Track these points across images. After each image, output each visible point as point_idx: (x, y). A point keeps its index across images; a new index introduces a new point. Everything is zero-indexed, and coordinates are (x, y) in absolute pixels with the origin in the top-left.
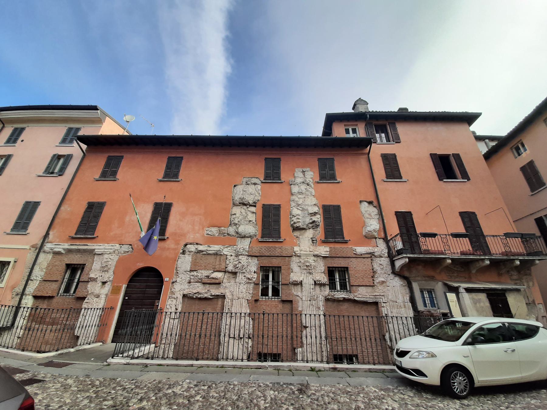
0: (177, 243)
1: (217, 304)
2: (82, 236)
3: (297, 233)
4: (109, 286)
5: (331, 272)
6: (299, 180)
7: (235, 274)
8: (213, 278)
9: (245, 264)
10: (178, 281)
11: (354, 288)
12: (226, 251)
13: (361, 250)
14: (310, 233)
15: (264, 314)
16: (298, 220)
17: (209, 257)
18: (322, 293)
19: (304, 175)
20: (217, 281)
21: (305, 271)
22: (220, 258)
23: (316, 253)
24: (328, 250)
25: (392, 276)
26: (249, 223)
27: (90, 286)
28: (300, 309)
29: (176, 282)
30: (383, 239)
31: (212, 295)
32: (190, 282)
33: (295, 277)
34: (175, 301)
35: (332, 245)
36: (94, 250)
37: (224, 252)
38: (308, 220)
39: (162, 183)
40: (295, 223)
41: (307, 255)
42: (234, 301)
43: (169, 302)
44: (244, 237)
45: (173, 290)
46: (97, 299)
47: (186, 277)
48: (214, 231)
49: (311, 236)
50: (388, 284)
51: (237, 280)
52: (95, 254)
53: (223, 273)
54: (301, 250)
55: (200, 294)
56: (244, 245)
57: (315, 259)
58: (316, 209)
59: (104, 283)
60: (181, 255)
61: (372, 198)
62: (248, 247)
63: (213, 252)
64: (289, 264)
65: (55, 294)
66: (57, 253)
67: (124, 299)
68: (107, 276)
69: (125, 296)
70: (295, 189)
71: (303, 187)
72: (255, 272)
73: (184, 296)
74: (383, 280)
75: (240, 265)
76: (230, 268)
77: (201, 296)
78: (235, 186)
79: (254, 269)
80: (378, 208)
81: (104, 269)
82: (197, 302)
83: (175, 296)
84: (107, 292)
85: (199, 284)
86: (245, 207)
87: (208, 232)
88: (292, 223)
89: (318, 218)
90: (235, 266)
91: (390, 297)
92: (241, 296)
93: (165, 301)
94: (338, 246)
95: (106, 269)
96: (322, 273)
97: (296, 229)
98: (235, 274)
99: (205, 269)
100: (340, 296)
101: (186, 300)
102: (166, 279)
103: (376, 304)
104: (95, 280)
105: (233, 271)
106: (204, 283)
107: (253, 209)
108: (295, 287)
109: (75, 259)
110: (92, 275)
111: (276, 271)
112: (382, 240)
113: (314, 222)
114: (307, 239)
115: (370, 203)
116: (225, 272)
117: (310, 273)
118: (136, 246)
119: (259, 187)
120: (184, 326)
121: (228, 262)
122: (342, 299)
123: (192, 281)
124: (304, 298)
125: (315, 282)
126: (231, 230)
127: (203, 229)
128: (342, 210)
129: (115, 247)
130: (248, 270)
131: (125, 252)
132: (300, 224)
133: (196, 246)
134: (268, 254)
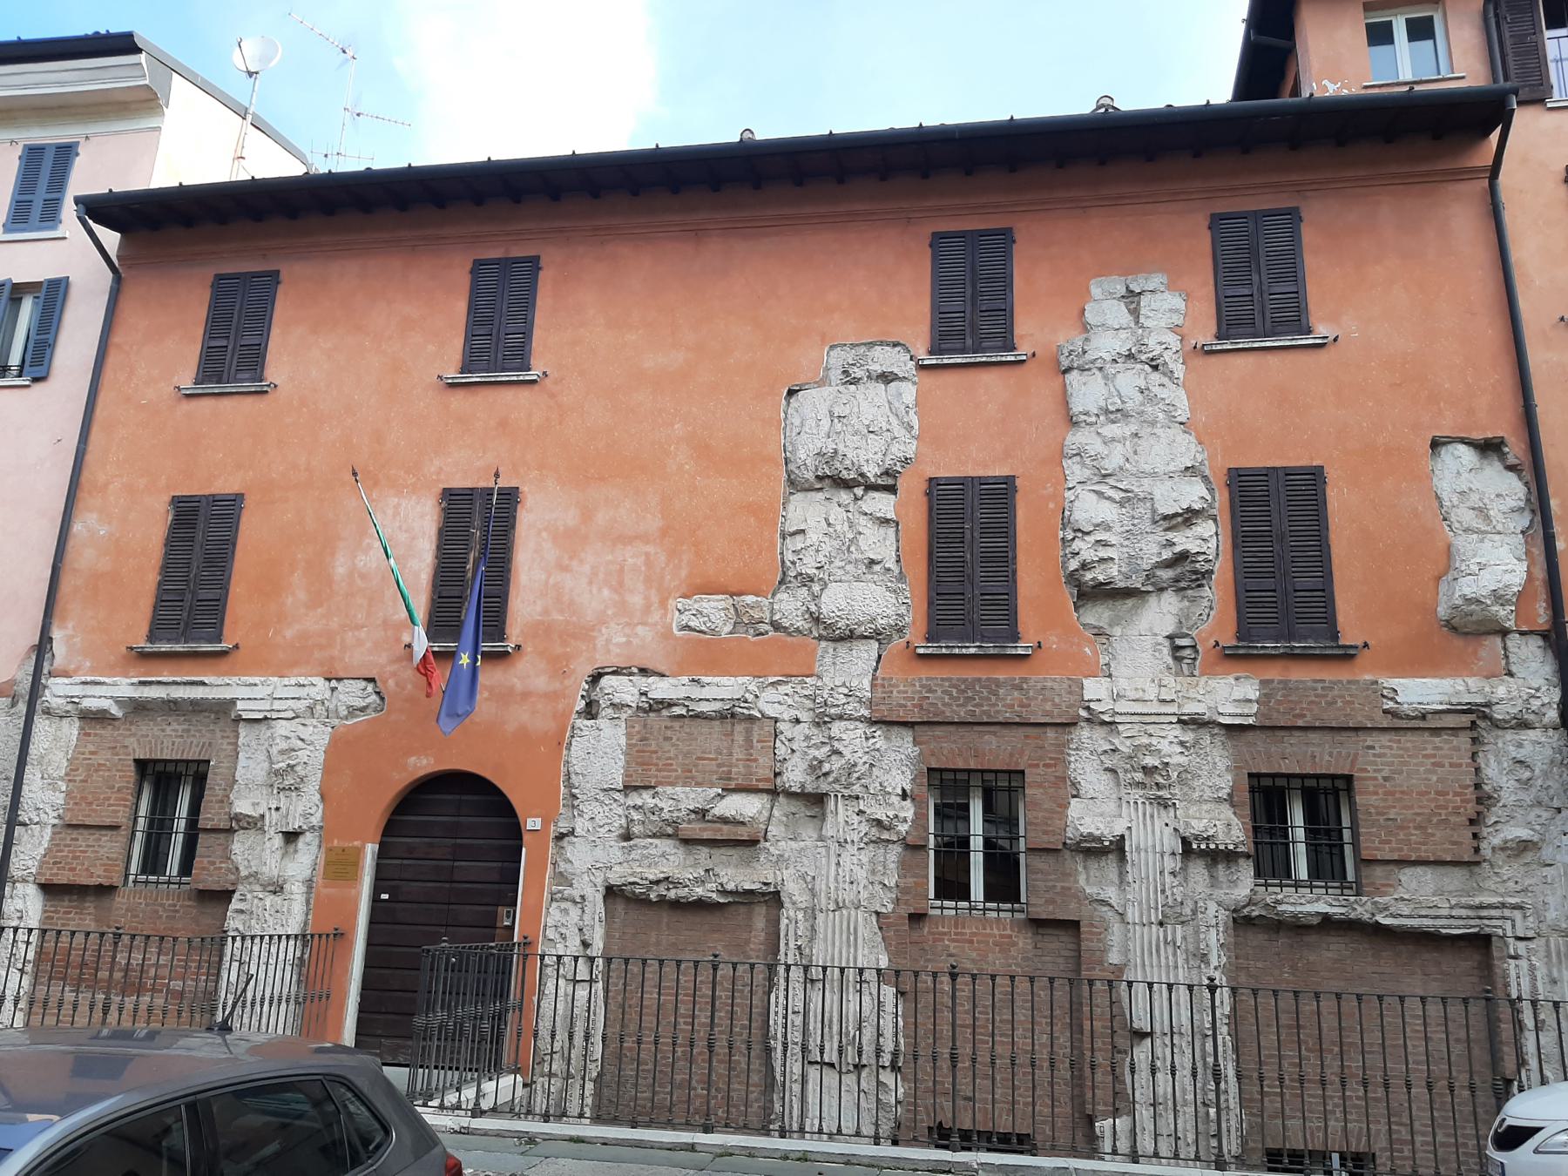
0: (559, 667)
1: (749, 928)
2: (178, 648)
3: (1096, 615)
4: (314, 848)
5: (1265, 798)
6: (1106, 345)
7: (816, 801)
8: (724, 820)
9: (861, 759)
10: (578, 831)
11: (1379, 871)
12: (772, 701)
13: (1420, 691)
14: (1162, 614)
15: (954, 977)
16: (1104, 553)
17: (704, 727)
18: (1219, 894)
19: (1135, 313)
20: (743, 833)
21: (1137, 794)
22: (748, 732)
23: (1191, 708)
24: (1254, 694)
26: (864, 570)
27: (240, 846)
28: (1114, 958)
29: (572, 833)
30: (1544, 636)
31: (724, 892)
32: (627, 837)
33: (1092, 814)
34: (575, 913)
35: (1274, 672)
36: (233, 702)
37: (761, 704)
38: (1151, 550)
39: (460, 394)
40: (1084, 566)
42: (821, 917)
43: (553, 915)
44: (849, 636)
45: (562, 866)
46: (278, 899)
47: (612, 814)
48: (714, 611)
49: (1170, 629)
50: (1547, 853)
51: (829, 830)
52: (239, 719)
53: (765, 798)
54: (1117, 697)
55: (677, 884)
56: (851, 671)
57: (1188, 737)
58: (1193, 494)
59: (291, 837)
60: (582, 723)
61: (1504, 425)
62: (866, 684)
63: (717, 706)
64: (1060, 761)
65: (117, 880)
66: (94, 719)
67: (375, 899)
68: (300, 809)
69: (376, 891)
70: (1087, 393)
71: (1129, 381)
72: (904, 796)
73: (611, 892)
74: (1524, 833)
75: (836, 764)
76: (795, 776)
77: (683, 892)
78: (791, 393)
79: (899, 778)
80: (1528, 475)
81: (283, 780)
82: (665, 916)
83: (576, 894)
84: (307, 873)
85: (665, 845)
86: (845, 496)
87: (685, 618)
88: (1073, 564)
90: (815, 768)
91: (1551, 915)
92: (848, 896)
93: (535, 914)
94: (1302, 674)
95: (289, 781)
96: (1219, 800)
97: (1092, 593)
98: (816, 801)
99: (689, 778)
100: (1309, 908)
101: (620, 907)
102: (532, 823)
103: (1481, 943)
104: (254, 824)
105: (809, 789)
106: (687, 842)
107: (882, 504)
108: (1093, 865)
109: (168, 742)
110: (242, 806)
111: (1002, 791)
112: (1535, 643)
113: (1183, 557)
114: (1148, 642)
115: (1489, 448)
116: (774, 793)
117: (1164, 804)
118: (391, 683)
119: (908, 392)
120: (620, 1010)
121: (782, 751)
122: (1316, 921)
123: (636, 829)
124: (1133, 914)
125: (1185, 842)
126: (790, 606)
127: (663, 603)
128: (1332, 494)
129: (312, 691)
131: (353, 711)
132: (1113, 571)
133: (642, 682)
134: (962, 714)
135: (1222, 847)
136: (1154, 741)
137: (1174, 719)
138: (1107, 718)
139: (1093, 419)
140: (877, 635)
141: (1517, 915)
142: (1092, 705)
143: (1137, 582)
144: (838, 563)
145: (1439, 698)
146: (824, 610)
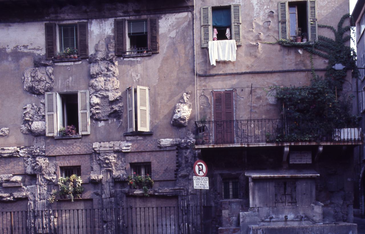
8: (13, 182)
16: (97, 111)
23: (116, 148)
90: (33, 168)
91: (190, 191)
135: (121, 180)
136: (108, 157)
137: (113, 151)
138: (98, 152)
139: (95, 76)
141: (183, 191)
142: (95, 149)
144: (35, 116)
145: (169, 143)
146: (32, 129)
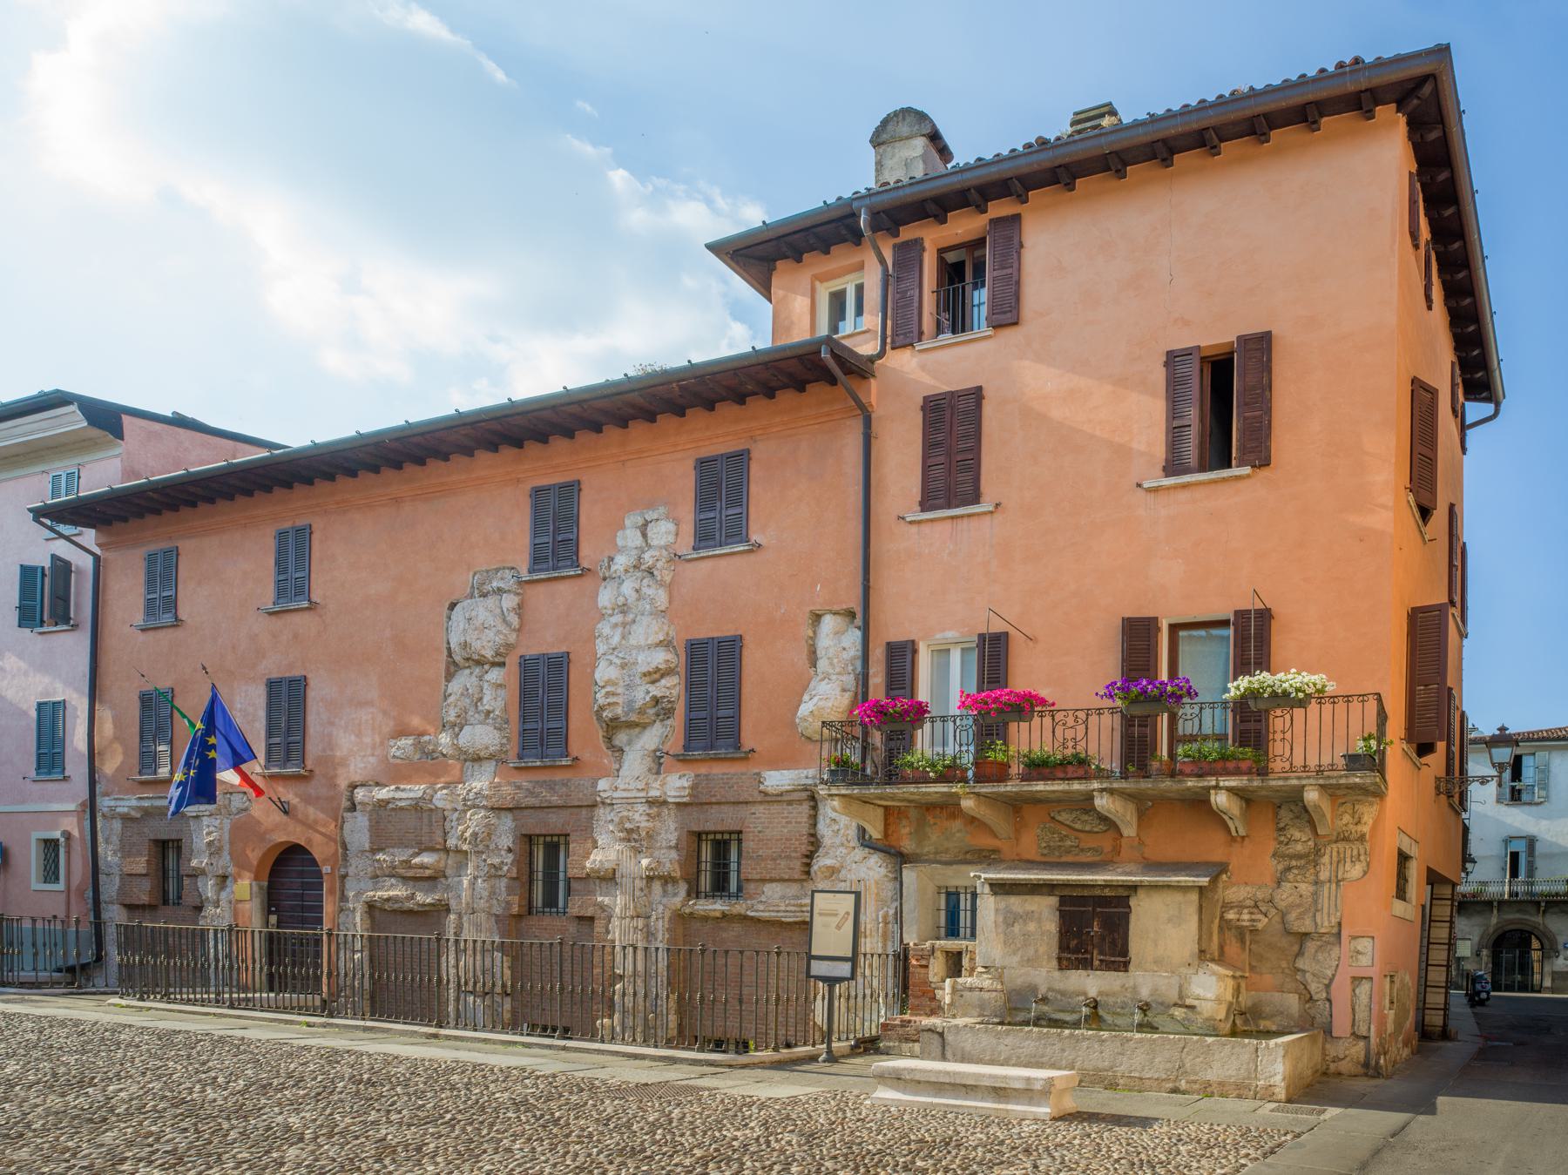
6: (621, 562)
12: (441, 799)
13: (777, 779)
16: (611, 700)
18: (665, 900)
23: (654, 793)
25: (860, 853)
35: (703, 769)
40: (602, 708)
41: (630, 803)
44: (478, 759)
56: (481, 782)
57: (654, 811)
58: (660, 658)
72: (510, 850)
79: (506, 841)
86: (477, 670)
89: (672, 687)
94: (718, 769)
102: (326, 869)
107: (495, 675)
111: (554, 847)
113: (656, 701)
128: (745, 653)
130: (492, 846)
132: (619, 711)
140: (491, 757)
143: (633, 717)
